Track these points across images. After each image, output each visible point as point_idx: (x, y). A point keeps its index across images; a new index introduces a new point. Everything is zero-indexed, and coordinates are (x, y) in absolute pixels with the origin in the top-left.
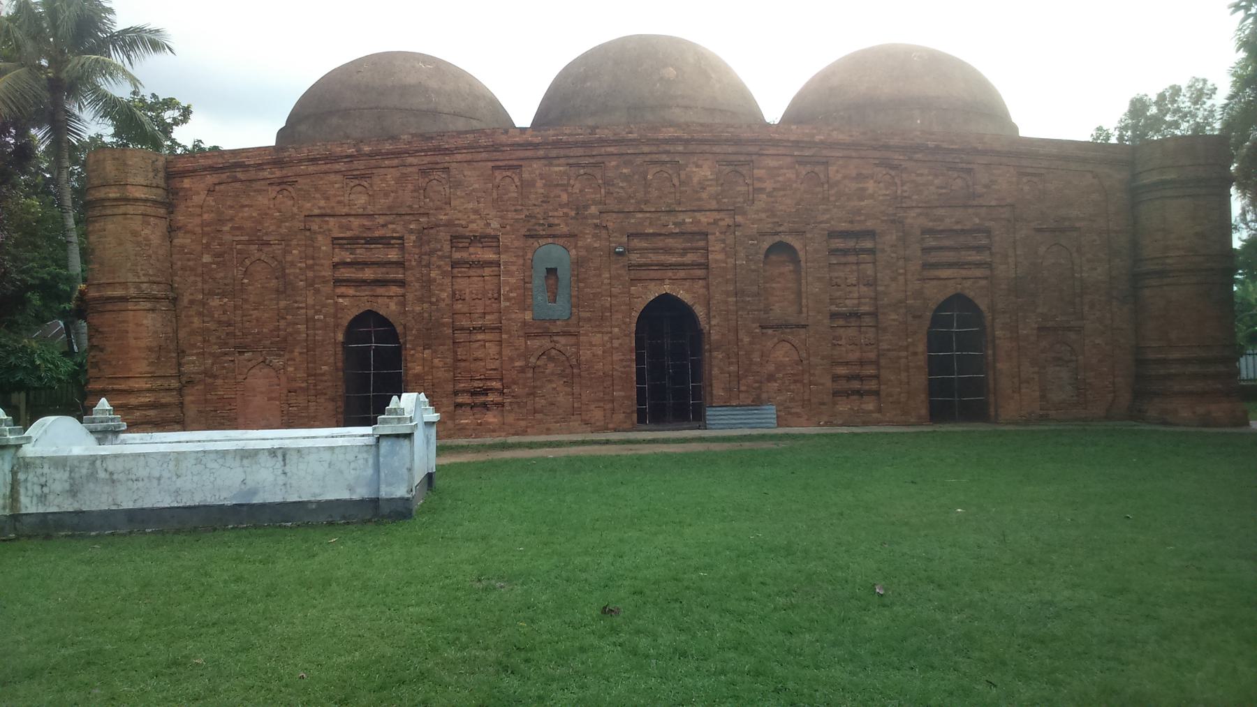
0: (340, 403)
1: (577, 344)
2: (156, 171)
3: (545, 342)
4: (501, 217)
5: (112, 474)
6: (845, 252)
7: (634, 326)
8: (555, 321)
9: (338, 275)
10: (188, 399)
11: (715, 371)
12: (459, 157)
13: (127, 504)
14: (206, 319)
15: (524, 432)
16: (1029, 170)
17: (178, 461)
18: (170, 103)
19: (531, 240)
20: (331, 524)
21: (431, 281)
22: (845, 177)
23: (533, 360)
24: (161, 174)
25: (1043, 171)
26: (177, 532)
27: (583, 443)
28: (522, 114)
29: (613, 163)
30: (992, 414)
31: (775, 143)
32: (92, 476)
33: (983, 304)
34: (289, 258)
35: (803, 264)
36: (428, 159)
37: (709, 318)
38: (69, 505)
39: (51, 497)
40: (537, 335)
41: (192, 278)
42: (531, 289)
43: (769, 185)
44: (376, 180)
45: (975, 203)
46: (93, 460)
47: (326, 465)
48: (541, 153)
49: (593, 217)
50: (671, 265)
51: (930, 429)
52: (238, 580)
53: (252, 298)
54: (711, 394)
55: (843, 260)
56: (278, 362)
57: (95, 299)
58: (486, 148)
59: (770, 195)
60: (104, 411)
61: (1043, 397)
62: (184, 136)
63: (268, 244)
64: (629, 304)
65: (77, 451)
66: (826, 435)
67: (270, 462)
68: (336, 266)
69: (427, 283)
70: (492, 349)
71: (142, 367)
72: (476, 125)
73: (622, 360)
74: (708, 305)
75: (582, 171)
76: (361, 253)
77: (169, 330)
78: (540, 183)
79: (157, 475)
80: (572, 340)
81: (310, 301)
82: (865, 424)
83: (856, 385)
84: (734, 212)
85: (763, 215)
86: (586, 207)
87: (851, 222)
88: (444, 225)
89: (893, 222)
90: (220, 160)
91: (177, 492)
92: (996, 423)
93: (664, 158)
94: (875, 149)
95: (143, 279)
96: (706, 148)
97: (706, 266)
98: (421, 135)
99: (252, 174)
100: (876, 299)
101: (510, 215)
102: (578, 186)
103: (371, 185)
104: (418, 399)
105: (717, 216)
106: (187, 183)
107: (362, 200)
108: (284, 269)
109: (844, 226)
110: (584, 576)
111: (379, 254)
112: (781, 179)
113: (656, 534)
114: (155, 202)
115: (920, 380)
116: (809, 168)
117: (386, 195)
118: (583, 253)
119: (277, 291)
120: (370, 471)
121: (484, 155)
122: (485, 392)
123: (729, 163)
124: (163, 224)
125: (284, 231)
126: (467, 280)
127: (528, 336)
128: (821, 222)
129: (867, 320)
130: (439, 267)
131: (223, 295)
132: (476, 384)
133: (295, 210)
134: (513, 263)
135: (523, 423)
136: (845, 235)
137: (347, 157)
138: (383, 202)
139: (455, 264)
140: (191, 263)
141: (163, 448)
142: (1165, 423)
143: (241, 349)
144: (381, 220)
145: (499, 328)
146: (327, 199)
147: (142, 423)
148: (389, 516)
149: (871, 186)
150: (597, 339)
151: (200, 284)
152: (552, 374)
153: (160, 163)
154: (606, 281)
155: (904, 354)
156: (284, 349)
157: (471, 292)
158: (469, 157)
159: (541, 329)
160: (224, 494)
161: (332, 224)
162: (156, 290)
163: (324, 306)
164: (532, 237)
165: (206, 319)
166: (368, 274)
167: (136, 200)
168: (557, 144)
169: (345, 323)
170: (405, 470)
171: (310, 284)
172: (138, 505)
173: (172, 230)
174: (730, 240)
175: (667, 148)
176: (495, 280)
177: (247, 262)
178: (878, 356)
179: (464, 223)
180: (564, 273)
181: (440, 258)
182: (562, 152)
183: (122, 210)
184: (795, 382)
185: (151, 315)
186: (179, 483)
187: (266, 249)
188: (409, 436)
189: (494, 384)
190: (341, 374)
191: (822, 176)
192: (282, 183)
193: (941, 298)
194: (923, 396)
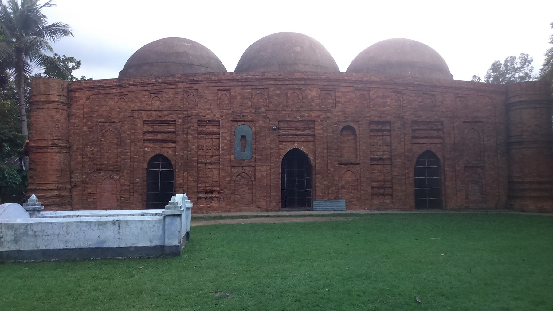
0: (144, 197)
1: (255, 171)
2: (63, 89)
3: (240, 170)
4: (221, 112)
5: (35, 232)
6: (377, 131)
7: (280, 163)
8: (244, 160)
9: (145, 137)
10: (74, 193)
11: (318, 184)
12: (202, 85)
13: (42, 247)
14: (84, 157)
15: (229, 211)
16: (460, 95)
17: (67, 226)
18: (71, 60)
19: (234, 123)
20: (141, 258)
21: (188, 141)
22: (377, 97)
23: (234, 178)
24: (66, 90)
25: (465, 96)
26: (66, 261)
27: (257, 216)
28: (231, 66)
29: (272, 89)
30: (444, 205)
31: (346, 81)
32: (26, 233)
33: (439, 155)
34: (123, 129)
35: (358, 136)
36: (187, 86)
37: (315, 158)
38: (14, 247)
39: (5, 243)
40: (236, 166)
41: (78, 138)
42: (234, 145)
43: (343, 100)
44: (164, 95)
45: (436, 109)
46: (26, 225)
47: (139, 230)
48: (240, 83)
49: (263, 112)
50: (298, 135)
51: (416, 212)
52: (96, 289)
53: (105, 147)
54: (316, 194)
55: (376, 134)
56: (116, 177)
57: (33, 147)
58: (215, 81)
59: (343, 104)
60: (33, 200)
61: (467, 198)
62: (77, 74)
63: (113, 122)
64: (279, 153)
65: (19, 221)
66: (368, 214)
67: (112, 227)
68: (144, 133)
69: (186, 142)
70: (216, 172)
71: (53, 178)
72: (210, 70)
73: (275, 178)
74: (314, 153)
75: (258, 92)
76: (156, 128)
77: (67, 162)
78: (239, 97)
79: (57, 232)
80: (252, 169)
81: (132, 149)
82: (386, 209)
83: (382, 192)
84: (327, 111)
85: (340, 113)
86: (260, 108)
87: (380, 117)
88: (195, 116)
89: (399, 117)
90: (93, 84)
91: (67, 242)
92: (445, 210)
93: (296, 86)
94: (391, 84)
95: (55, 138)
96: (315, 83)
97: (314, 136)
98: (186, 75)
99: (107, 91)
100: (391, 152)
101: (225, 111)
102: (256, 98)
103: (162, 97)
104: (183, 196)
105: (320, 113)
106: (77, 94)
107: (158, 103)
108: (120, 134)
109: (376, 119)
110: (269, 290)
111: (164, 128)
112: (348, 97)
113: (300, 266)
114: (62, 102)
115: (411, 189)
116: (361, 92)
117: (169, 101)
118: (259, 129)
119: (117, 144)
120: (160, 233)
121: (214, 84)
122: (212, 192)
123: (325, 90)
124: (66, 113)
125: (121, 117)
126: (204, 141)
127: (232, 167)
128: (366, 117)
129: (387, 162)
130: (192, 134)
131: (92, 146)
132: (208, 188)
133: (127, 107)
134: (226, 133)
135: (229, 207)
136: (377, 123)
137: (151, 84)
138: (167, 105)
139: (199, 133)
140: (77, 131)
141: (60, 220)
142: (523, 211)
143: (100, 171)
144: (166, 113)
145: (219, 163)
146: (142, 103)
147: (53, 205)
148: (169, 255)
149: (389, 100)
150: (264, 168)
151: (81, 141)
152: (243, 184)
153: (65, 85)
154: (268, 142)
155: (404, 177)
156: (119, 171)
157: (206, 146)
158: (207, 85)
159: (238, 163)
160: (90, 243)
161: (143, 114)
162: (61, 143)
163: (138, 151)
164: (235, 121)
165: (84, 157)
166: (159, 137)
167: (54, 102)
168: (247, 80)
169: (148, 159)
170: (177, 232)
171: (133, 142)
172: (48, 248)
173: (70, 116)
174: (325, 124)
175: (297, 82)
176: (218, 141)
177: (104, 131)
178: (392, 178)
179: (204, 114)
180: (249, 138)
181: (193, 130)
182: (249, 83)
183: (46, 106)
184: (354, 189)
185: (58, 155)
186: (68, 237)
187: (112, 125)
188: (179, 216)
189: (216, 189)
190: (145, 183)
191: (367, 96)
192: (121, 95)
193: (420, 152)
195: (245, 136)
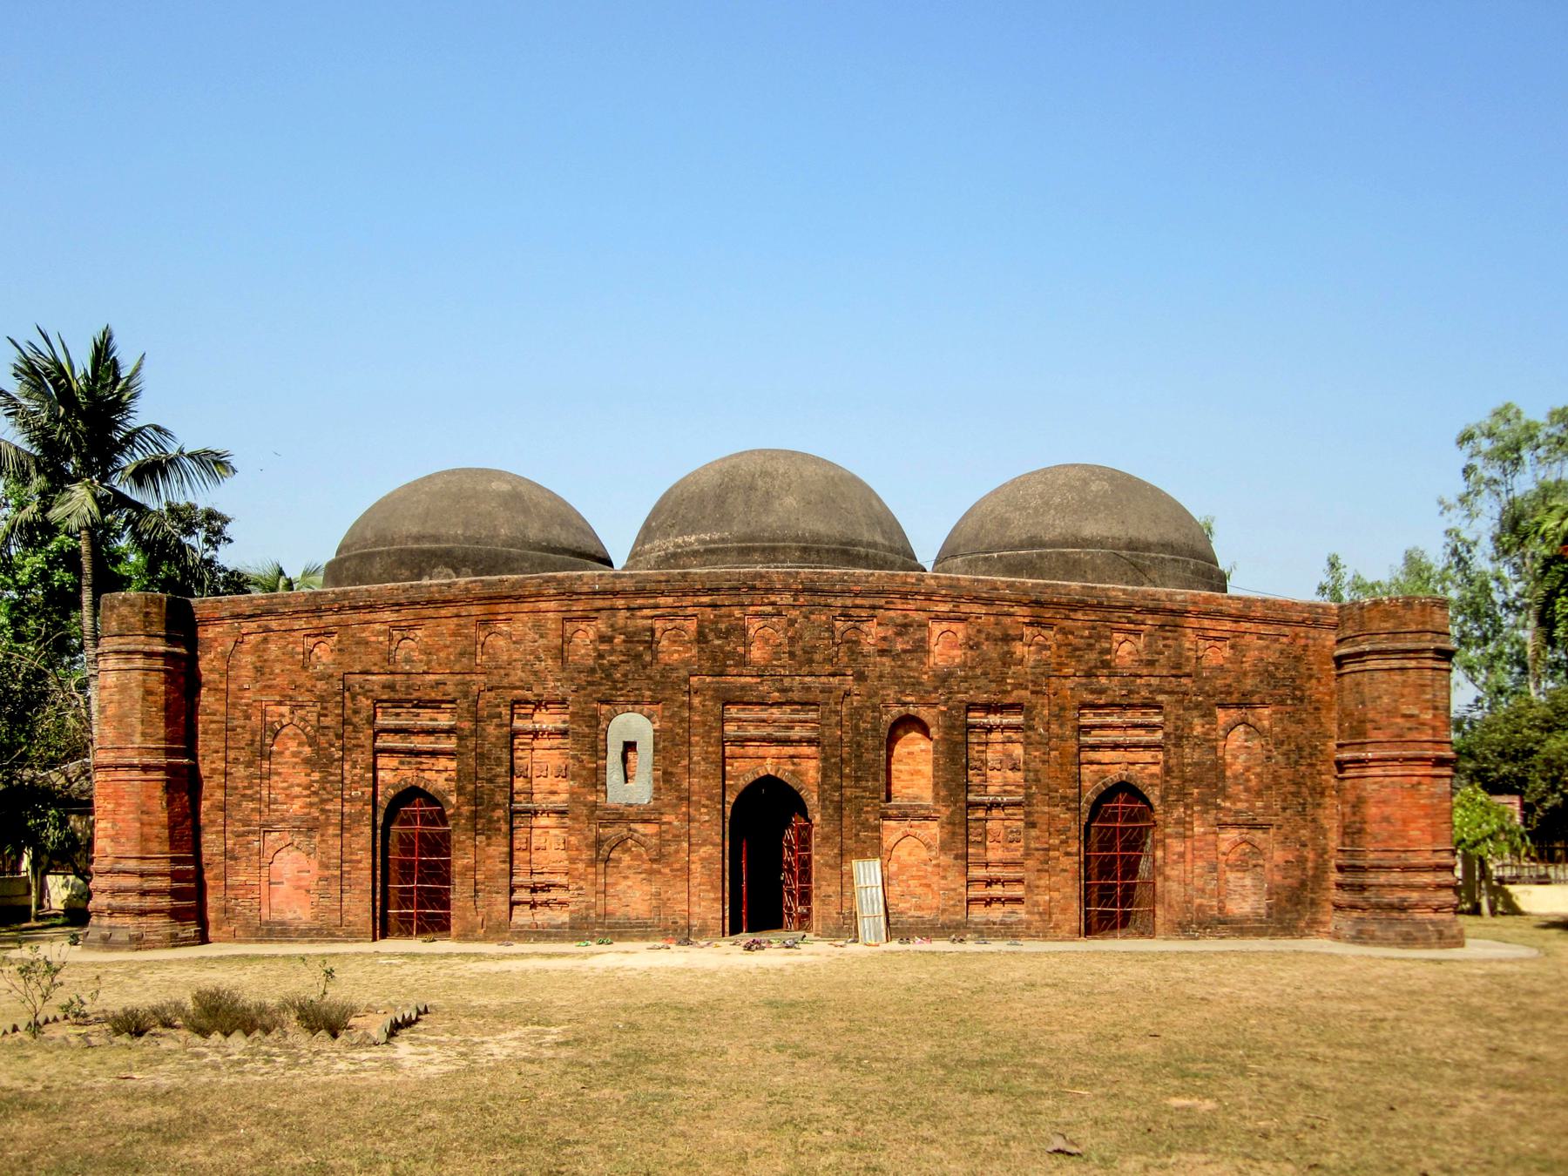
12: (526, 607)
93: (769, 609)
116: (945, 625)
122: (547, 888)
132: (536, 878)
152: (629, 867)
175: (773, 598)
189: (558, 879)
194: (1076, 905)
195: (634, 744)
